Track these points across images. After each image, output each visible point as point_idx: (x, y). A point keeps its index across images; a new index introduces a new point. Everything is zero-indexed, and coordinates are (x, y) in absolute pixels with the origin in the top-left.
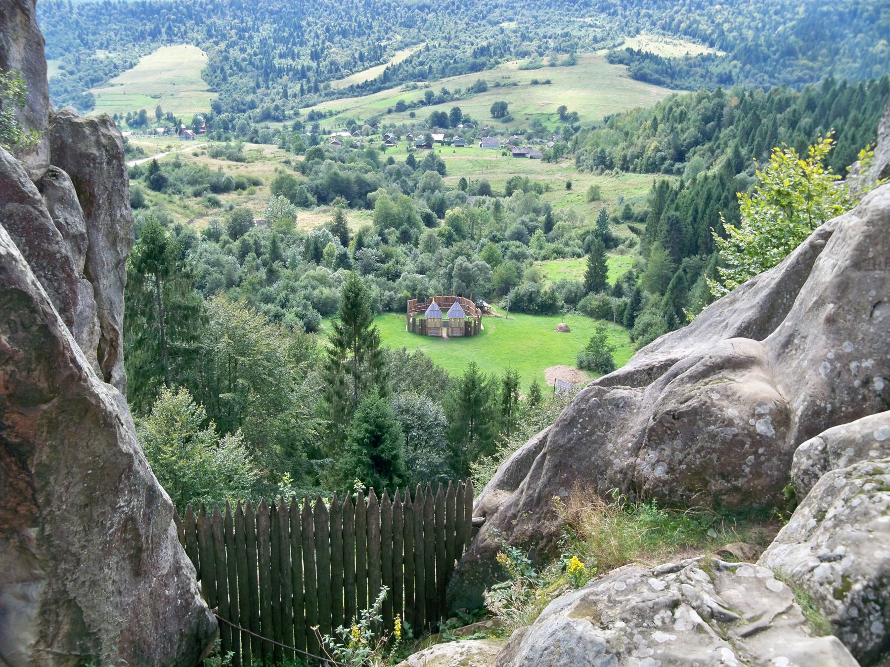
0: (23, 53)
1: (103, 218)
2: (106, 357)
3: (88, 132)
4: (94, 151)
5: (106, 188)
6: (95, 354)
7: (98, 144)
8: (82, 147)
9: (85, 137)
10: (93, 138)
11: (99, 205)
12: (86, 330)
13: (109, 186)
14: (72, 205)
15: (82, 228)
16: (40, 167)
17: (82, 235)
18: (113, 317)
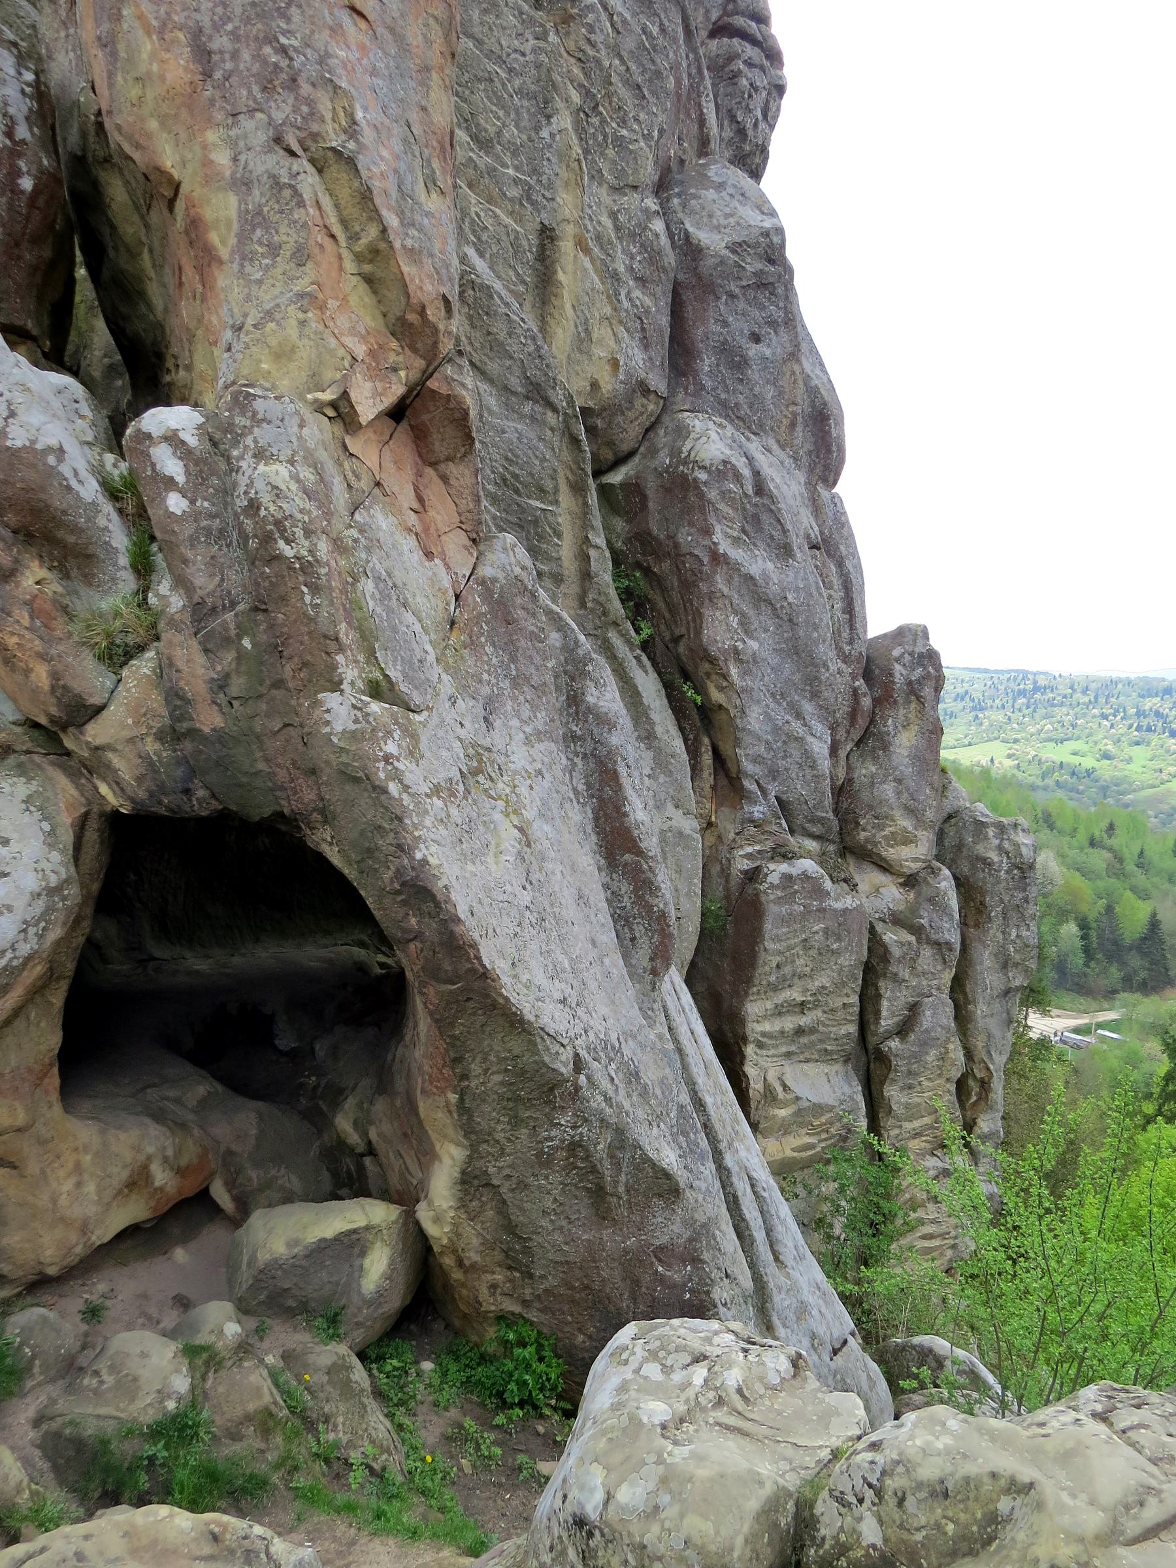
0: (914, 742)
1: (994, 931)
2: (974, 1098)
3: (991, 834)
4: (994, 856)
5: (1002, 901)
6: (953, 1088)
7: (1000, 848)
8: (980, 849)
9: (986, 838)
10: (997, 842)
11: (990, 918)
12: (933, 1052)
13: (1006, 899)
14: (944, 909)
15: (954, 938)
16: (915, 860)
17: (949, 946)
18: (989, 1052)
